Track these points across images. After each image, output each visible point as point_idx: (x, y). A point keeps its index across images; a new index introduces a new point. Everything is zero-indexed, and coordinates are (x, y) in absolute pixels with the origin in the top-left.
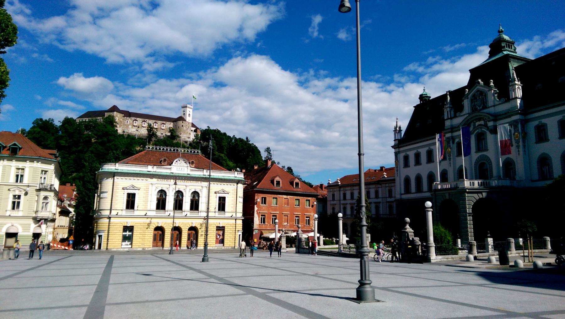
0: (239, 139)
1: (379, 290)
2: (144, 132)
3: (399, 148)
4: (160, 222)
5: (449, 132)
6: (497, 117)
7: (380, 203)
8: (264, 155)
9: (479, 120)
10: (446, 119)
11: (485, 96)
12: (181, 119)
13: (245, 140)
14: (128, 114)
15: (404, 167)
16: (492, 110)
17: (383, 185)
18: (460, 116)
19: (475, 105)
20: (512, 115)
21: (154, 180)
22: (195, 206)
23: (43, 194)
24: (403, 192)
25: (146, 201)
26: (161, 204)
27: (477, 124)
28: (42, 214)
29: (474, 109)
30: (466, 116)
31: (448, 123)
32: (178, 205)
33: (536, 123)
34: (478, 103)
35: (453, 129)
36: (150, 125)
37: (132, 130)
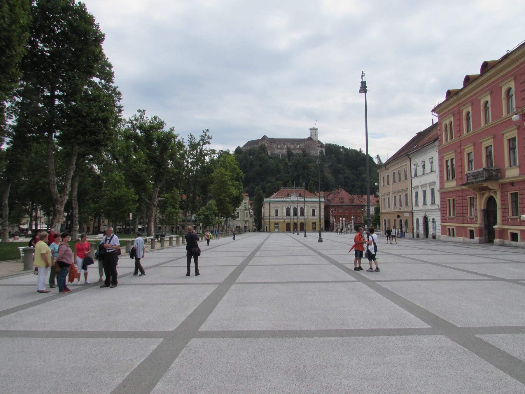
0: (354, 150)
2: (285, 151)
4: (288, 221)
8: (376, 162)
12: (310, 139)
13: (359, 150)
14: (274, 141)
21: (284, 204)
22: (302, 214)
23: (246, 212)
25: (282, 212)
26: (288, 214)
28: (246, 219)
32: (295, 214)
36: (288, 148)
37: (277, 151)
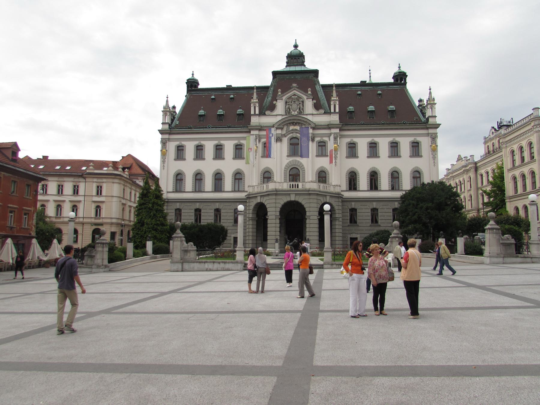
1: (404, 307)
3: (170, 134)
5: (256, 129)
6: (316, 127)
7: (80, 201)
9: (294, 124)
10: (253, 115)
11: (303, 102)
15: (175, 160)
16: (310, 118)
17: (87, 180)
18: (269, 115)
19: (289, 108)
20: (333, 128)
24: (171, 189)
27: (291, 128)
29: (288, 111)
30: (280, 118)
31: (255, 121)
33: (348, 140)
34: (294, 106)
35: (260, 128)
